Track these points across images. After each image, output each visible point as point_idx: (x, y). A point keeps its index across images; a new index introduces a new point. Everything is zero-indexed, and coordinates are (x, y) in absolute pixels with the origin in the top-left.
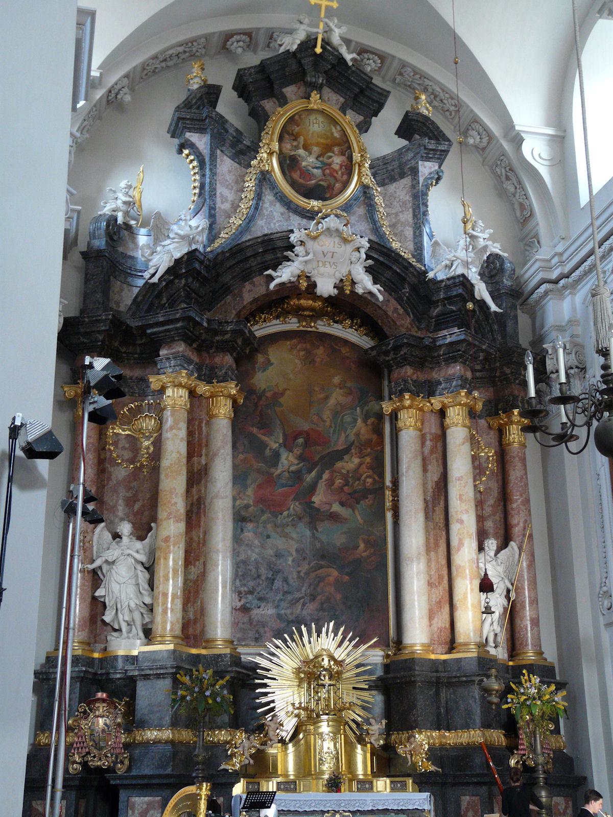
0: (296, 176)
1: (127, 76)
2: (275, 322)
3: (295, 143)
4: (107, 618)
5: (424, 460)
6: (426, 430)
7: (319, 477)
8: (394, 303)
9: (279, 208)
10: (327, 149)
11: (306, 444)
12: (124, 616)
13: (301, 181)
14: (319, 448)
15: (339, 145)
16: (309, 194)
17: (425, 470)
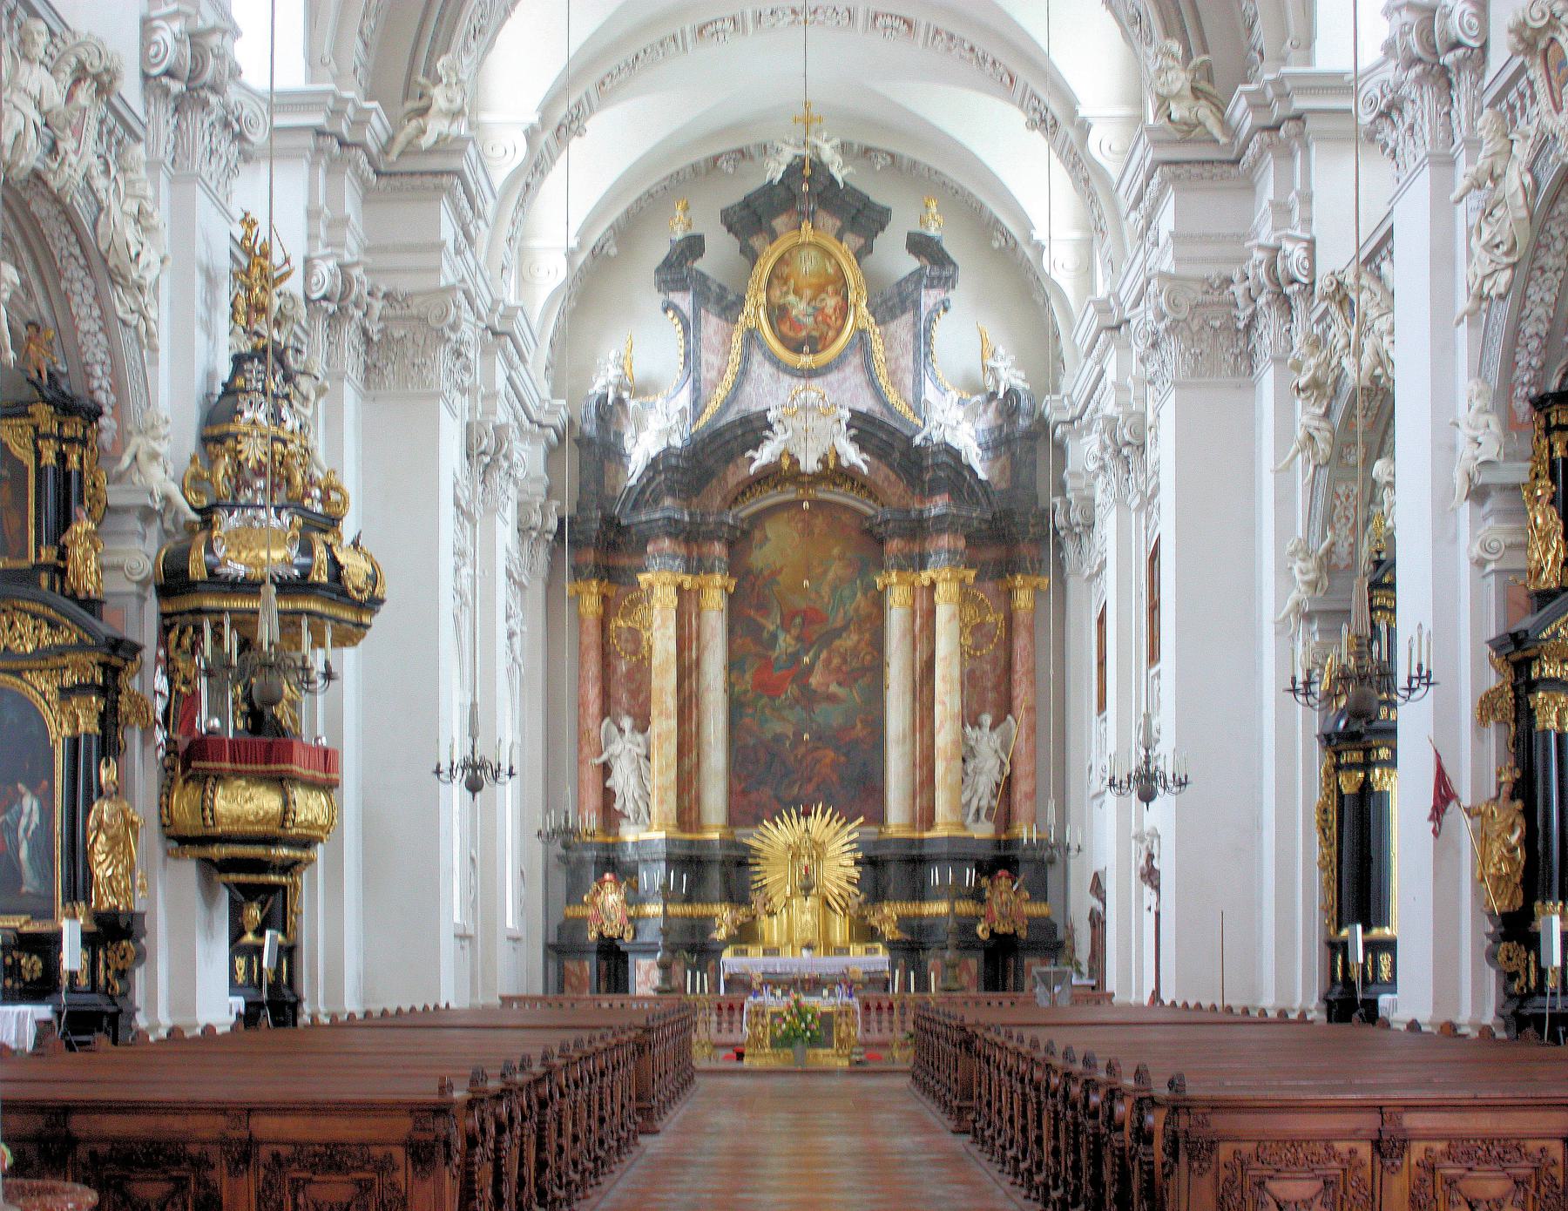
0: (785, 328)
1: (611, 227)
2: (771, 492)
3: (785, 289)
4: (618, 806)
5: (914, 637)
7: (817, 657)
8: (884, 470)
10: (820, 289)
12: (630, 807)
13: (791, 334)
14: (816, 627)
15: (833, 283)
16: (797, 349)
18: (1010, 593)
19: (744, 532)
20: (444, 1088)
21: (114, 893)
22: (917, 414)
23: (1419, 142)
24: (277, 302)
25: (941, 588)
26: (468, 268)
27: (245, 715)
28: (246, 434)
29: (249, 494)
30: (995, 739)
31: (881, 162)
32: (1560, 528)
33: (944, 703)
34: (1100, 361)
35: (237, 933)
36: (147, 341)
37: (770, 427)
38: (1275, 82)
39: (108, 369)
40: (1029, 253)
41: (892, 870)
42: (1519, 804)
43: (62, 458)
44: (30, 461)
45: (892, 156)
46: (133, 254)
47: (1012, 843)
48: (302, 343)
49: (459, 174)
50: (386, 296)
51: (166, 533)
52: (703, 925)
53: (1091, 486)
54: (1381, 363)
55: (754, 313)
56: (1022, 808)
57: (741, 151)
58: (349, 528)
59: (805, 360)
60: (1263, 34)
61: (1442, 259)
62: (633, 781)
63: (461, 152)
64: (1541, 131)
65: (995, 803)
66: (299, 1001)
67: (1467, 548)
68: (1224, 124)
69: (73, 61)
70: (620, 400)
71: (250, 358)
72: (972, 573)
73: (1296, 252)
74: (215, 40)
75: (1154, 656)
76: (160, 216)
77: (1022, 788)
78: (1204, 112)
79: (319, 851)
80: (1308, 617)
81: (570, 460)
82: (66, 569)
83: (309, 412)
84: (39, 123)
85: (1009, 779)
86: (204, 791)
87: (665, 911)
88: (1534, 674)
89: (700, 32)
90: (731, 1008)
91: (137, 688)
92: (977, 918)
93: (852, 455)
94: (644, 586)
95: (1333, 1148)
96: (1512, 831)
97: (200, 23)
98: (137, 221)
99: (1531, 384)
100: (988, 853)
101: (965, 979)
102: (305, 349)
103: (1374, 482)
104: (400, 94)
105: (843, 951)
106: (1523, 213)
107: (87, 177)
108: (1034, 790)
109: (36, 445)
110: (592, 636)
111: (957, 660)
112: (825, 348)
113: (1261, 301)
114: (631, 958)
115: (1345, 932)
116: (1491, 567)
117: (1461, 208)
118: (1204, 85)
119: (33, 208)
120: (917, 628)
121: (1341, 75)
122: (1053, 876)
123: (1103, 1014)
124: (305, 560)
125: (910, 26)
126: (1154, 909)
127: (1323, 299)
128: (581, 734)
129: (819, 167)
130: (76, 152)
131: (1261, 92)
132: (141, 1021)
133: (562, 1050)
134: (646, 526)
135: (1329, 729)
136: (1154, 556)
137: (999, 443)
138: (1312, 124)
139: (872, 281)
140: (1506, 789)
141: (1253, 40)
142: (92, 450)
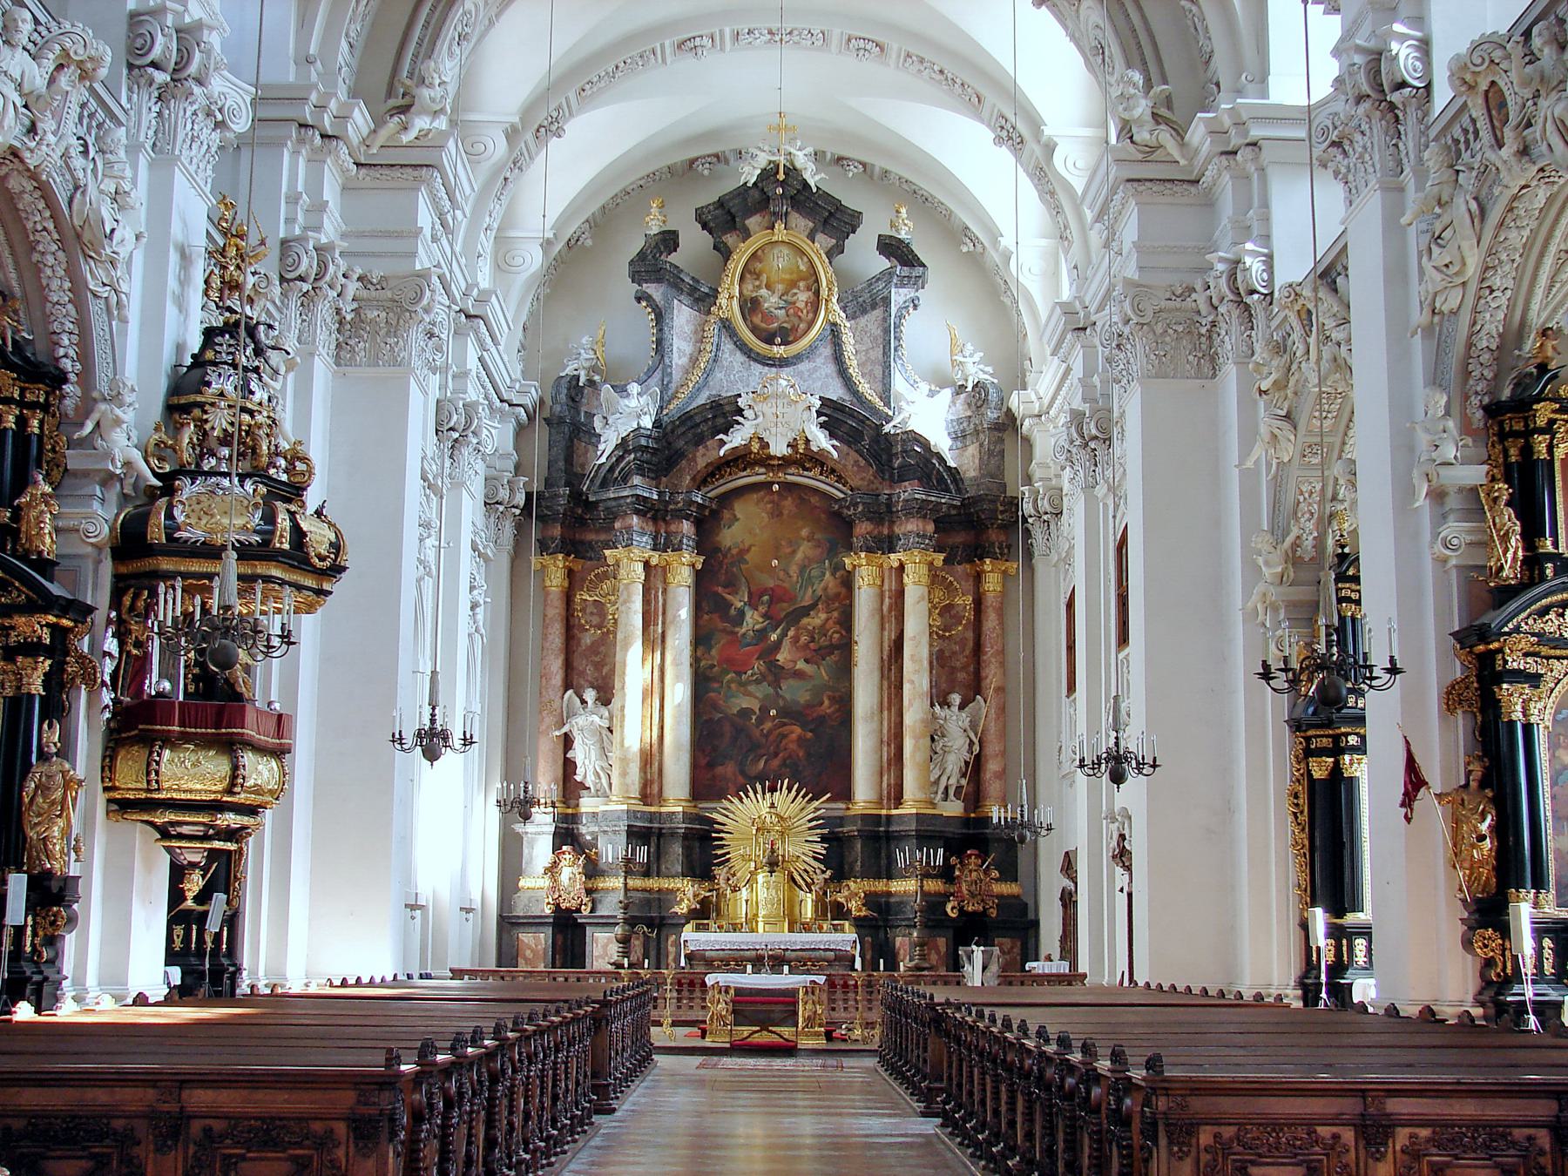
0: (757, 320)
3: (757, 283)
4: (578, 778)
5: (882, 618)
6: (886, 587)
7: (784, 634)
9: (740, 357)
10: (793, 284)
11: (771, 602)
13: (764, 325)
14: (785, 605)
17: (883, 629)
18: (978, 578)
19: (713, 512)
20: (393, 1059)
22: (888, 404)
23: (1371, 170)
24: (251, 280)
25: (909, 568)
26: (444, 253)
28: (213, 404)
29: (213, 462)
30: (964, 718)
31: (853, 171)
32: (1518, 529)
33: (912, 682)
37: (740, 412)
39: (75, 339)
43: (22, 421)
45: (864, 165)
46: (108, 231)
48: (275, 320)
51: (125, 498)
53: (1058, 476)
56: (993, 788)
57: (717, 156)
58: (313, 497)
59: (779, 351)
60: (1221, 66)
65: (964, 782)
66: (239, 970)
71: (221, 331)
72: (942, 556)
73: (1255, 265)
75: (1123, 639)
76: (139, 195)
77: (992, 767)
78: (1165, 136)
81: (540, 436)
82: (18, 530)
83: (277, 386)
84: (19, 104)
85: (978, 757)
86: (151, 753)
87: (626, 884)
89: (679, 47)
91: (86, 650)
92: (946, 896)
93: (821, 441)
94: (610, 561)
95: (1315, 1132)
96: (1484, 820)
97: (187, 20)
101: (934, 957)
102: (277, 324)
104: (383, 96)
105: (807, 928)
107: (65, 156)
108: (1004, 770)
110: (556, 609)
111: (925, 639)
112: (795, 340)
120: (885, 608)
125: (882, 49)
126: (1125, 890)
129: (792, 171)
133: (515, 1023)
134: (614, 503)
139: (841, 277)
141: (1209, 74)
142: (54, 416)
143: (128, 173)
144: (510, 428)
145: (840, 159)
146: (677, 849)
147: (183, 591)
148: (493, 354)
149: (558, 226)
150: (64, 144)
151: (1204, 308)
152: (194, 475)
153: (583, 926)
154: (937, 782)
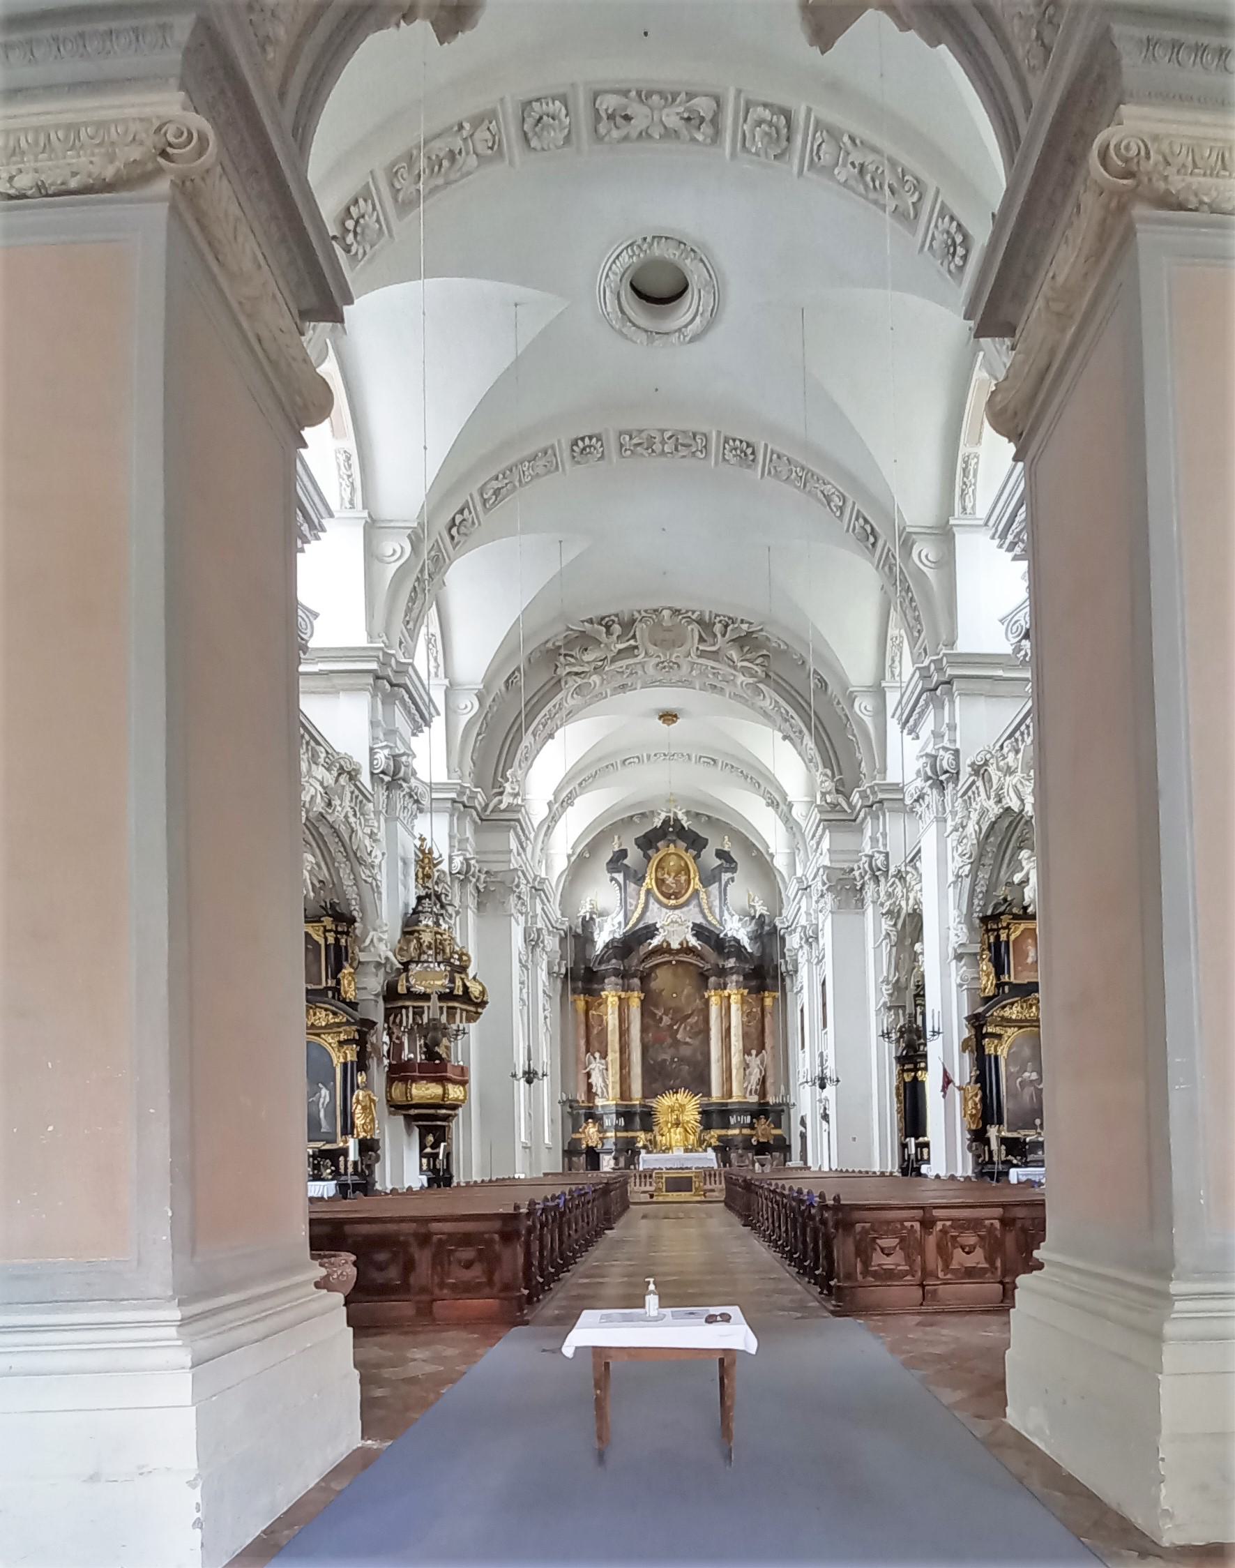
0: (664, 889)
4: (594, 1090)
9: (657, 905)
12: (599, 1092)
16: (669, 898)
18: (762, 999)
21: (365, 1131)
24: (436, 874)
25: (733, 997)
27: (425, 1053)
28: (424, 931)
29: (426, 956)
31: (704, 819)
34: (799, 903)
35: (422, 1147)
36: (376, 890)
37: (657, 929)
38: (870, 787)
40: (768, 858)
41: (714, 1116)
42: (979, 1085)
43: (337, 940)
44: (322, 942)
47: (767, 1103)
49: (518, 820)
50: (487, 872)
51: (387, 973)
52: (633, 1141)
53: (796, 955)
54: (917, 903)
55: (650, 882)
58: (471, 971)
59: (672, 902)
61: (942, 861)
62: (600, 1080)
63: (519, 811)
64: (982, 806)
67: (955, 980)
68: (849, 804)
69: (338, 765)
70: (591, 918)
74: (404, 759)
75: (825, 1026)
76: (381, 835)
78: (841, 800)
79: (460, 1111)
80: (889, 1009)
81: (570, 942)
83: (452, 922)
88: (984, 1031)
90: (645, 1177)
92: (752, 1136)
93: (693, 942)
98: (370, 837)
99: (980, 912)
100: (756, 1107)
103: (915, 952)
106: (975, 842)
107: (346, 817)
109: (324, 933)
110: (582, 1018)
113: (866, 878)
114: (601, 1155)
115: (908, 1139)
116: (965, 987)
117: (949, 840)
118: (841, 788)
119: (321, 830)
121: (898, 784)
122: (783, 1118)
123: (806, 1174)
124: (452, 985)
127: (892, 877)
128: (577, 1059)
129: (677, 820)
130: (340, 805)
131: (865, 791)
132: (378, 1187)
135: (899, 1054)
136: (824, 984)
137: (756, 937)
138: (886, 804)
140: (973, 1079)
143: (376, 824)
144: (557, 940)
145: (698, 814)
146: (637, 1119)
147: (414, 1013)
148: (548, 907)
149: (574, 848)
150: (345, 811)
151: (858, 878)
152: (417, 963)
153: (598, 1154)
154: (747, 1088)
